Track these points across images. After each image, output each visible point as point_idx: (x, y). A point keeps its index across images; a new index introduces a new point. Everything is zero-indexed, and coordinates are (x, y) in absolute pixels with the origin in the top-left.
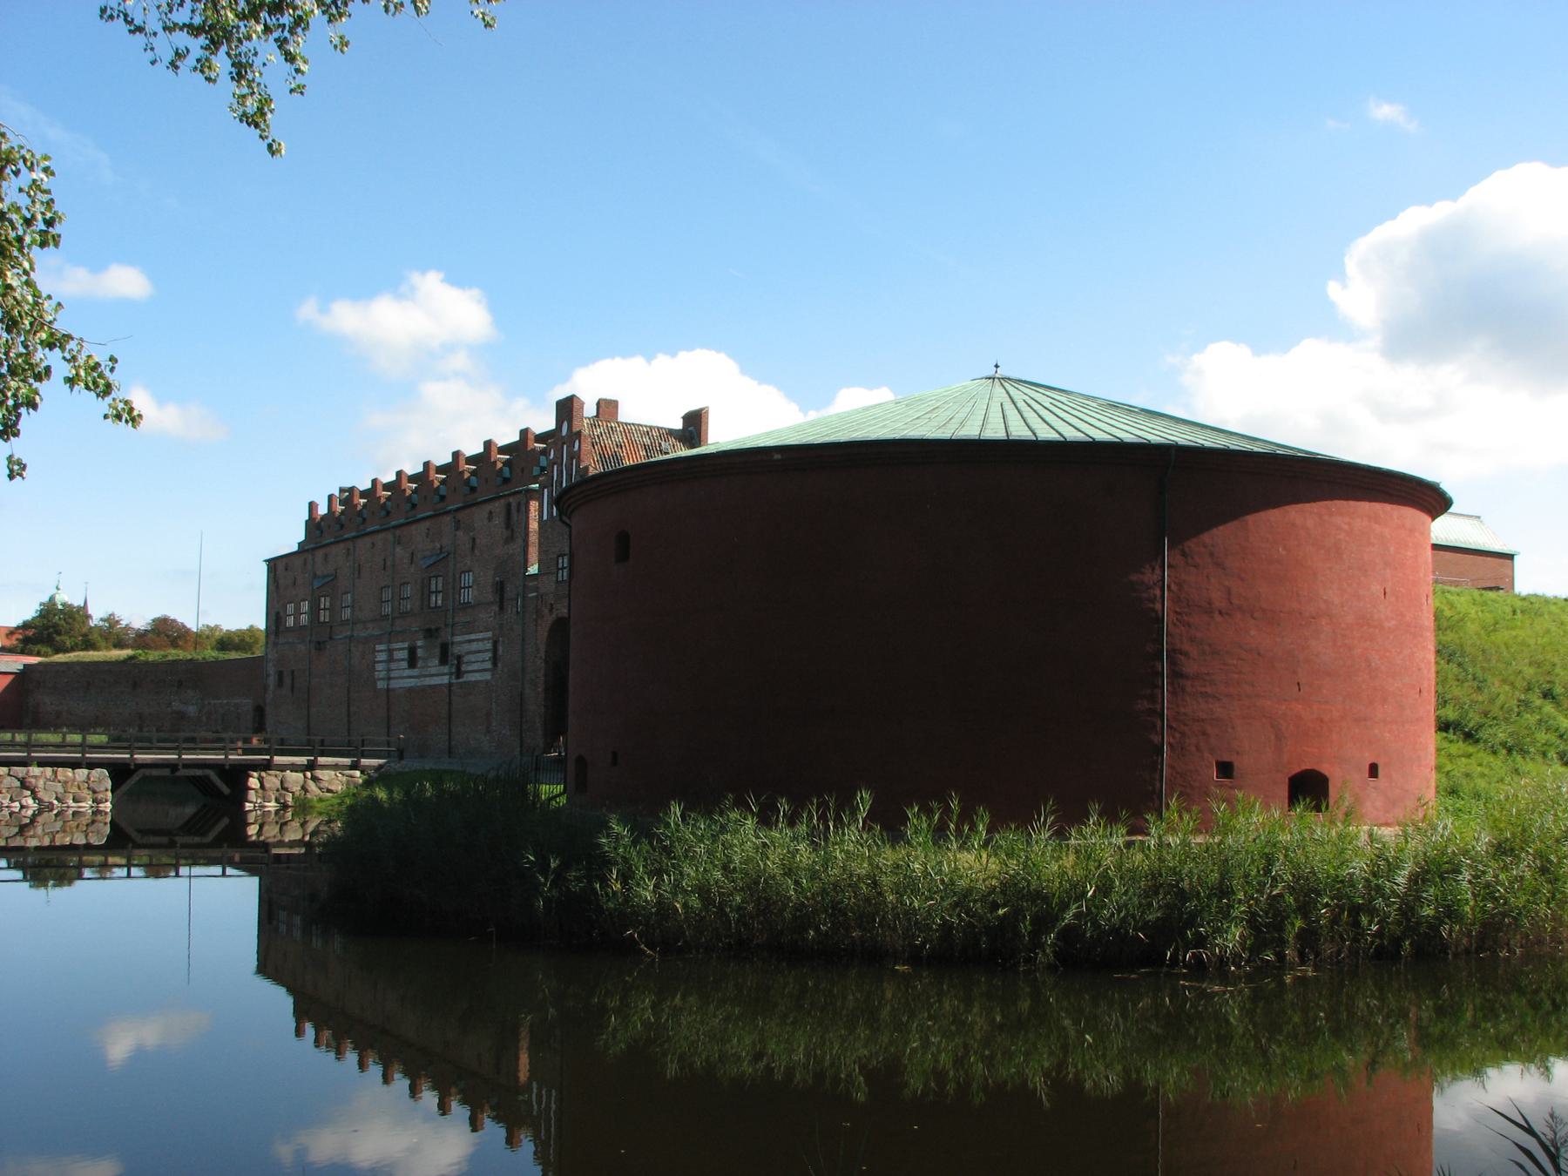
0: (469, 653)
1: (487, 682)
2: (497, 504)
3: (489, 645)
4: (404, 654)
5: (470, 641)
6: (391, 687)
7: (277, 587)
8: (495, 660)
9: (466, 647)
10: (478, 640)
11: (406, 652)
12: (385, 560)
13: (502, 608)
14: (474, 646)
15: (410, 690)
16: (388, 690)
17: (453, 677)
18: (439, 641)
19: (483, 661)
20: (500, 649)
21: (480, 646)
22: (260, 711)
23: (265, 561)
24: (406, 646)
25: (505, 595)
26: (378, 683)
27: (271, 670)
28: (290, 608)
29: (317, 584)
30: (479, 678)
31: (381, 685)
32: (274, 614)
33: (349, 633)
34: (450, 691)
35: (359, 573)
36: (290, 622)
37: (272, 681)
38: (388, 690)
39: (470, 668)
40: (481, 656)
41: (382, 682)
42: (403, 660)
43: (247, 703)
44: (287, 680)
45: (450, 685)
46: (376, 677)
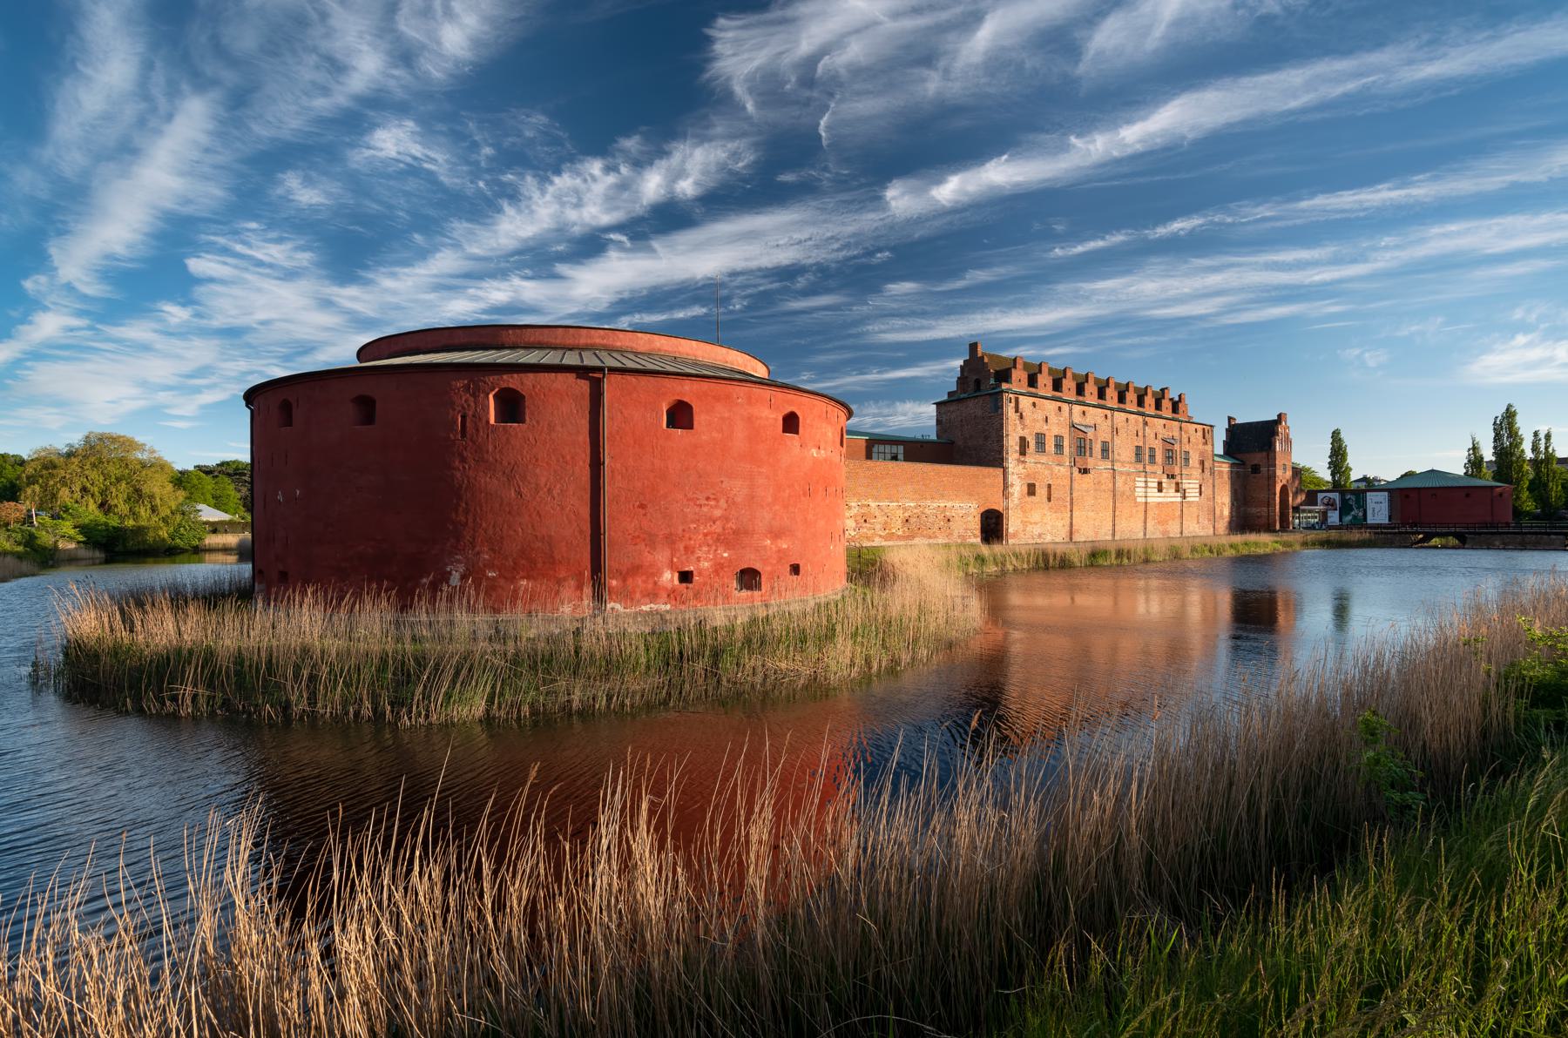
3: (1198, 486)
4: (1156, 485)
7: (1021, 417)
14: (1191, 486)
15: (1159, 503)
16: (1146, 503)
31: (1139, 500)
32: (1018, 440)
38: (1146, 503)
44: (1041, 491)
46: (1136, 494)
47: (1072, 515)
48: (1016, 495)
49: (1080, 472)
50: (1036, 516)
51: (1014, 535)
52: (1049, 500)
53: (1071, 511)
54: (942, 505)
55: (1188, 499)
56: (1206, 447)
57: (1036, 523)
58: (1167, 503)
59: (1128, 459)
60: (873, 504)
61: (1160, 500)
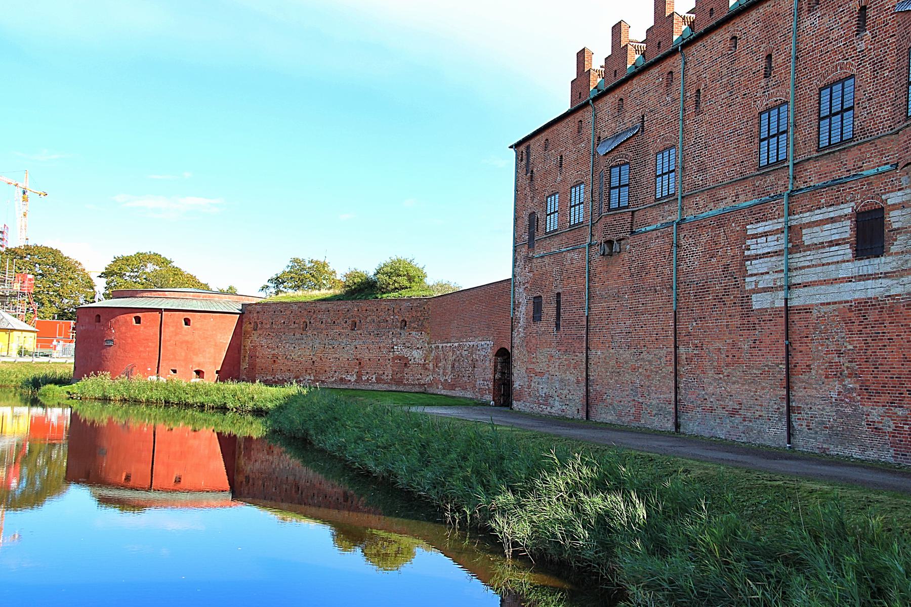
4: (846, 230)
6: (795, 303)
11: (848, 223)
15: (862, 306)
22: (504, 356)
24: (847, 209)
26: (754, 297)
27: (523, 297)
28: (554, 203)
29: (602, 150)
31: (759, 302)
33: (676, 217)
35: (697, 103)
36: (552, 223)
37: (523, 312)
41: (767, 296)
42: (836, 243)
43: (485, 348)
44: (549, 310)
52: (558, 326)
53: (587, 348)
54: (471, 344)
57: (541, 374)
59: (733, 173)
60: (440, 345)
61: (873, 289)
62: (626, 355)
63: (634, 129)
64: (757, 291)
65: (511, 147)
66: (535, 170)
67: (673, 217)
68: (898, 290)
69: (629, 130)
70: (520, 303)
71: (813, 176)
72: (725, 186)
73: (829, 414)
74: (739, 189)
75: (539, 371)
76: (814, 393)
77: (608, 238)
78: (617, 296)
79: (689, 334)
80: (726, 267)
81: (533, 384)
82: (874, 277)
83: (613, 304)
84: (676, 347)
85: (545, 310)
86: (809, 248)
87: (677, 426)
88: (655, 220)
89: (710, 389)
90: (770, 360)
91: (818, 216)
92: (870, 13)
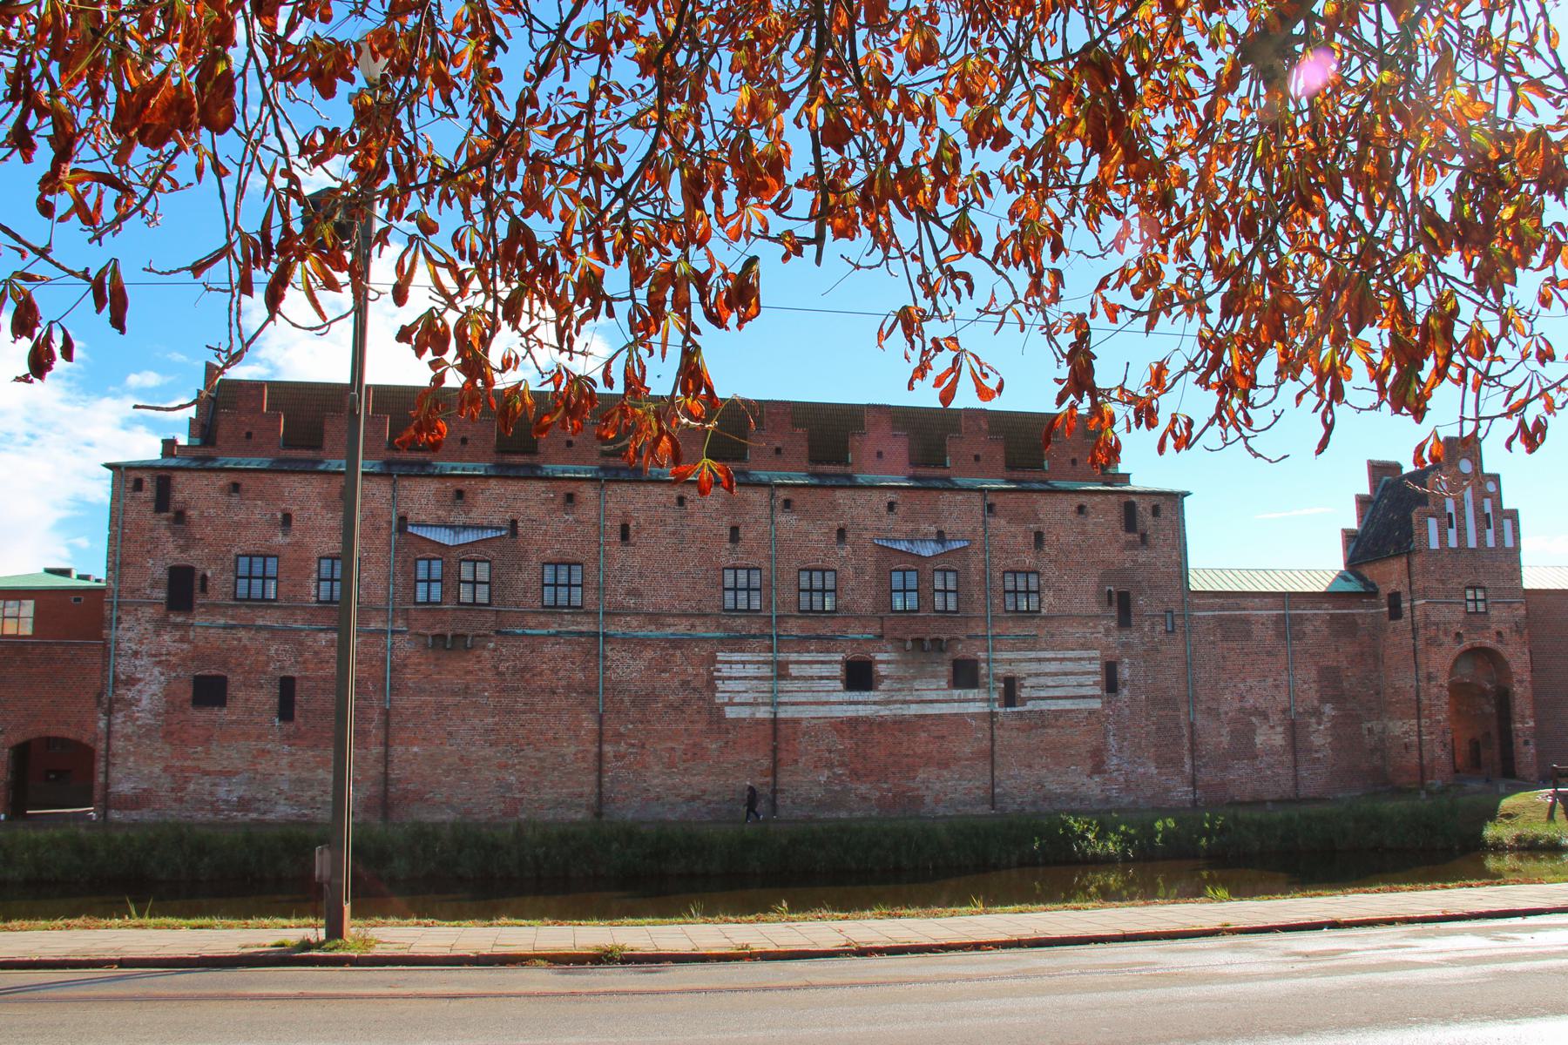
0: (1037, 675)
1: (1091, 712)
2: (1097, 499)
3: (1096, 666)
4: (837, 670)
5: (1040, 660)
6: (779, 716)
8: (1111, 683)
9: (1034, 667)
10: (1070, 659)
12: (734, 530)
13: (1125, 620)
14: (1053, 667)
15: (854, 722)
16: (775, 721)
17: (997, 705)
18: (948, 655)
19: (1080, 686)
20: (1125, 673)
21: (1069, 666)
23: (109, 466)
24: (839, 657)
25: (1133, 610)
26: (727, 709)
30: (1073, 707)
32: (161, 573)
34: (992, 723)
38: (775, 721)
39: (1043, 694)
40: (1072, 680)
42: (827, 678)
45: (993, 714)
46: (720, 698)
47: (386, 755)
48: (145, 702)
49: (426, 646)
50: (229, 755)
51: (136, 802)
53: (386, 744)
55: (1030, 706)
56: (1143, 556)
57: (228, 774)
58: (901, 723)
61: (863, 711)
62: (488, 752)
63: (499, 529)
64: (726, 704)
65: (109, 466)
66: (193, 514)
67: (584, 628)
68: (884, 711)
69: (482, 528)
70: (131, 681)
71: (794, 628)
72: (674, 616)
73: (818, 793)
74: (697, 622)
75: (219, 768)
76: (800, 778)
77: (460, 631)
78: (465, 692)
79: (621, 735)
80: (685, 684)
81: (191, 787)
82: (865, 703)
83: (450, 700)
84: (600, 747)
85: (237, 693)
86: (796, 678)
87: (599, 815)
88: (542, 625)
89: (656, 781)
90: (747, 757)
91: (806, 657)
92: (850, 537)
